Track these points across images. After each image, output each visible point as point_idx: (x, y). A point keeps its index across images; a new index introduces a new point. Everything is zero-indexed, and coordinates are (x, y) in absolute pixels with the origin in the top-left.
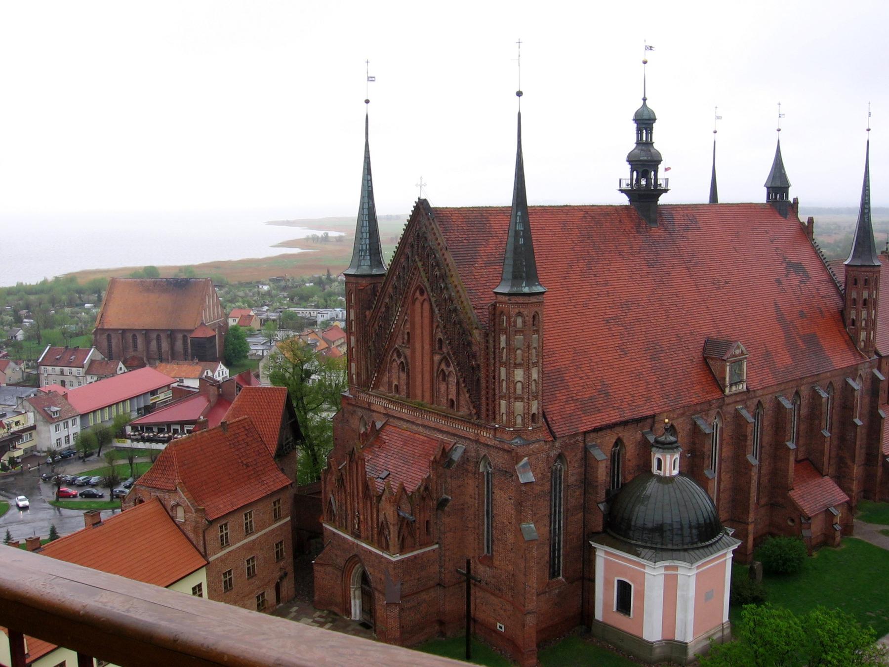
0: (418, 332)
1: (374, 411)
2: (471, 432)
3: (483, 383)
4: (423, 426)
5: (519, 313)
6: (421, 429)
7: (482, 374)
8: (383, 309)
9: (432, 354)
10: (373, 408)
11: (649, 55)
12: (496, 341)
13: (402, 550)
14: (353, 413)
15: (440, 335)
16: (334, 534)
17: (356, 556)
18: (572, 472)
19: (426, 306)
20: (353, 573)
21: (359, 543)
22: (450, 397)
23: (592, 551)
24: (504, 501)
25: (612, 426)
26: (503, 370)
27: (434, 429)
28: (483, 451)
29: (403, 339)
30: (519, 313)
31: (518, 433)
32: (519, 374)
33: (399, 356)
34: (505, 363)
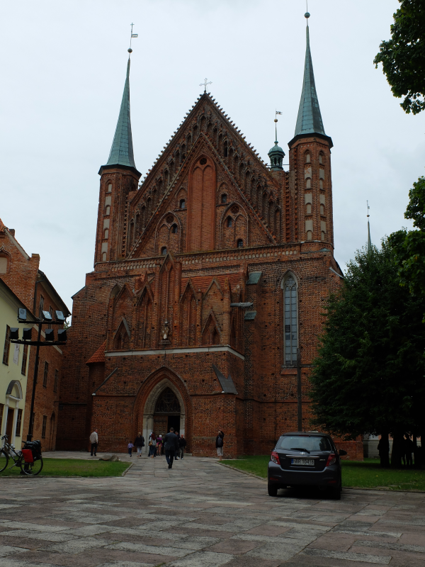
1: (132, 276)
4: (202, 269)
5: (321, 151)
6: (201, 274)
9: (217, 206)
10: (131, 273)
11: (278, 117)
15: (224, 191)
16: (124, 358)
17: (163, 369)
20: (149, 396)
21: (168, 352)
22: (237, 238)
27: (218, 268)
29: (176, 206)
30: (321, 151)
34: (309, 189)
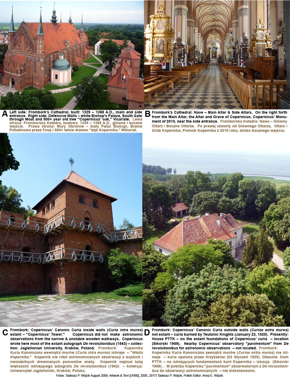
0: (22, 40)
2: (32, 55)
3: (34, 47)
7: (34, 46)
8: (15, 37)
12: (37, 42)
13: (20, 74)
14: (9, 53)
18: (48, 59)
19: (24, 37)
23: (51, 70)
24: (38, 64)
25: (53, 53)
26: (38, 46)
28: (34, 58)
31: (40, 55)
32: (41, 46)
33: (18, 44)
